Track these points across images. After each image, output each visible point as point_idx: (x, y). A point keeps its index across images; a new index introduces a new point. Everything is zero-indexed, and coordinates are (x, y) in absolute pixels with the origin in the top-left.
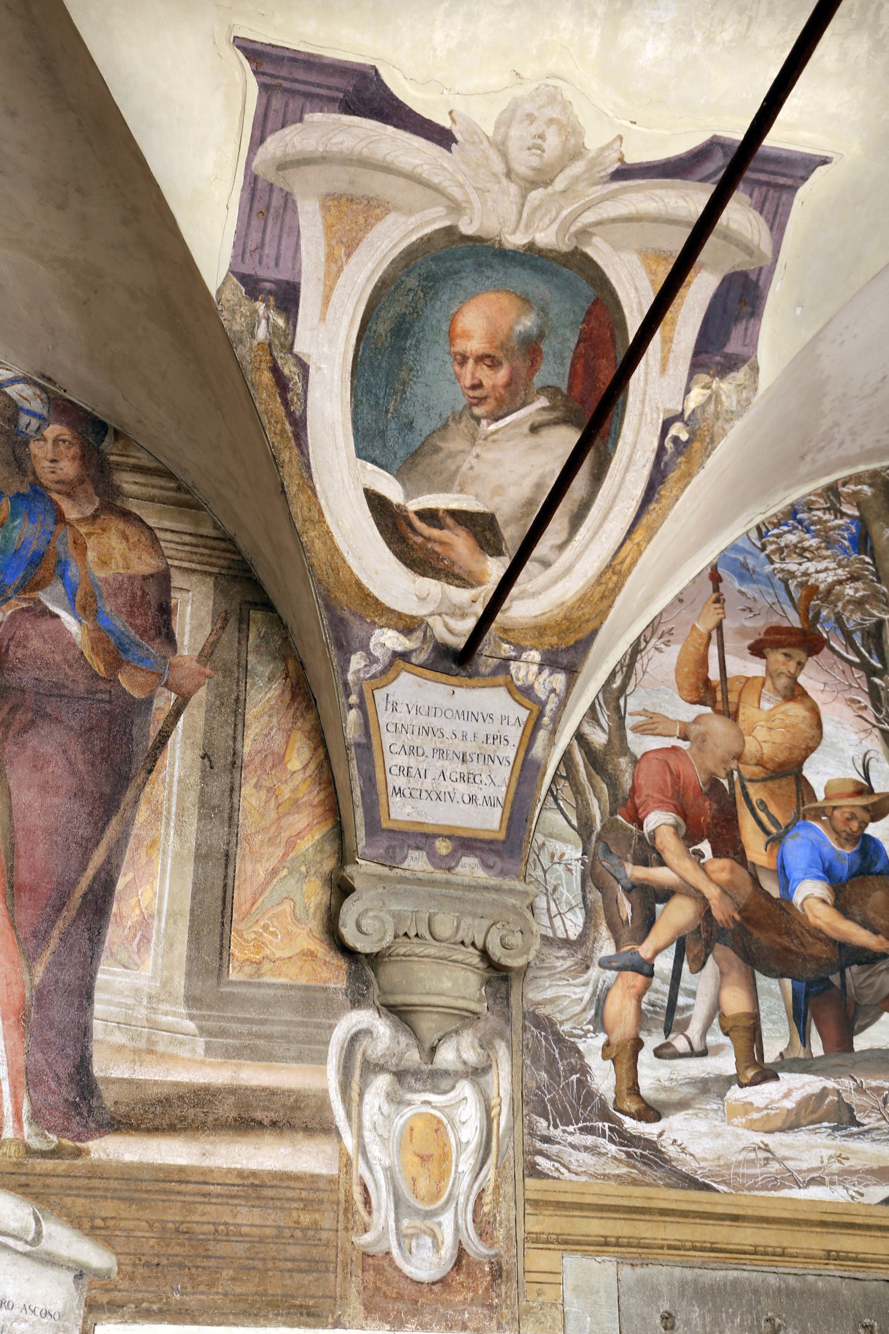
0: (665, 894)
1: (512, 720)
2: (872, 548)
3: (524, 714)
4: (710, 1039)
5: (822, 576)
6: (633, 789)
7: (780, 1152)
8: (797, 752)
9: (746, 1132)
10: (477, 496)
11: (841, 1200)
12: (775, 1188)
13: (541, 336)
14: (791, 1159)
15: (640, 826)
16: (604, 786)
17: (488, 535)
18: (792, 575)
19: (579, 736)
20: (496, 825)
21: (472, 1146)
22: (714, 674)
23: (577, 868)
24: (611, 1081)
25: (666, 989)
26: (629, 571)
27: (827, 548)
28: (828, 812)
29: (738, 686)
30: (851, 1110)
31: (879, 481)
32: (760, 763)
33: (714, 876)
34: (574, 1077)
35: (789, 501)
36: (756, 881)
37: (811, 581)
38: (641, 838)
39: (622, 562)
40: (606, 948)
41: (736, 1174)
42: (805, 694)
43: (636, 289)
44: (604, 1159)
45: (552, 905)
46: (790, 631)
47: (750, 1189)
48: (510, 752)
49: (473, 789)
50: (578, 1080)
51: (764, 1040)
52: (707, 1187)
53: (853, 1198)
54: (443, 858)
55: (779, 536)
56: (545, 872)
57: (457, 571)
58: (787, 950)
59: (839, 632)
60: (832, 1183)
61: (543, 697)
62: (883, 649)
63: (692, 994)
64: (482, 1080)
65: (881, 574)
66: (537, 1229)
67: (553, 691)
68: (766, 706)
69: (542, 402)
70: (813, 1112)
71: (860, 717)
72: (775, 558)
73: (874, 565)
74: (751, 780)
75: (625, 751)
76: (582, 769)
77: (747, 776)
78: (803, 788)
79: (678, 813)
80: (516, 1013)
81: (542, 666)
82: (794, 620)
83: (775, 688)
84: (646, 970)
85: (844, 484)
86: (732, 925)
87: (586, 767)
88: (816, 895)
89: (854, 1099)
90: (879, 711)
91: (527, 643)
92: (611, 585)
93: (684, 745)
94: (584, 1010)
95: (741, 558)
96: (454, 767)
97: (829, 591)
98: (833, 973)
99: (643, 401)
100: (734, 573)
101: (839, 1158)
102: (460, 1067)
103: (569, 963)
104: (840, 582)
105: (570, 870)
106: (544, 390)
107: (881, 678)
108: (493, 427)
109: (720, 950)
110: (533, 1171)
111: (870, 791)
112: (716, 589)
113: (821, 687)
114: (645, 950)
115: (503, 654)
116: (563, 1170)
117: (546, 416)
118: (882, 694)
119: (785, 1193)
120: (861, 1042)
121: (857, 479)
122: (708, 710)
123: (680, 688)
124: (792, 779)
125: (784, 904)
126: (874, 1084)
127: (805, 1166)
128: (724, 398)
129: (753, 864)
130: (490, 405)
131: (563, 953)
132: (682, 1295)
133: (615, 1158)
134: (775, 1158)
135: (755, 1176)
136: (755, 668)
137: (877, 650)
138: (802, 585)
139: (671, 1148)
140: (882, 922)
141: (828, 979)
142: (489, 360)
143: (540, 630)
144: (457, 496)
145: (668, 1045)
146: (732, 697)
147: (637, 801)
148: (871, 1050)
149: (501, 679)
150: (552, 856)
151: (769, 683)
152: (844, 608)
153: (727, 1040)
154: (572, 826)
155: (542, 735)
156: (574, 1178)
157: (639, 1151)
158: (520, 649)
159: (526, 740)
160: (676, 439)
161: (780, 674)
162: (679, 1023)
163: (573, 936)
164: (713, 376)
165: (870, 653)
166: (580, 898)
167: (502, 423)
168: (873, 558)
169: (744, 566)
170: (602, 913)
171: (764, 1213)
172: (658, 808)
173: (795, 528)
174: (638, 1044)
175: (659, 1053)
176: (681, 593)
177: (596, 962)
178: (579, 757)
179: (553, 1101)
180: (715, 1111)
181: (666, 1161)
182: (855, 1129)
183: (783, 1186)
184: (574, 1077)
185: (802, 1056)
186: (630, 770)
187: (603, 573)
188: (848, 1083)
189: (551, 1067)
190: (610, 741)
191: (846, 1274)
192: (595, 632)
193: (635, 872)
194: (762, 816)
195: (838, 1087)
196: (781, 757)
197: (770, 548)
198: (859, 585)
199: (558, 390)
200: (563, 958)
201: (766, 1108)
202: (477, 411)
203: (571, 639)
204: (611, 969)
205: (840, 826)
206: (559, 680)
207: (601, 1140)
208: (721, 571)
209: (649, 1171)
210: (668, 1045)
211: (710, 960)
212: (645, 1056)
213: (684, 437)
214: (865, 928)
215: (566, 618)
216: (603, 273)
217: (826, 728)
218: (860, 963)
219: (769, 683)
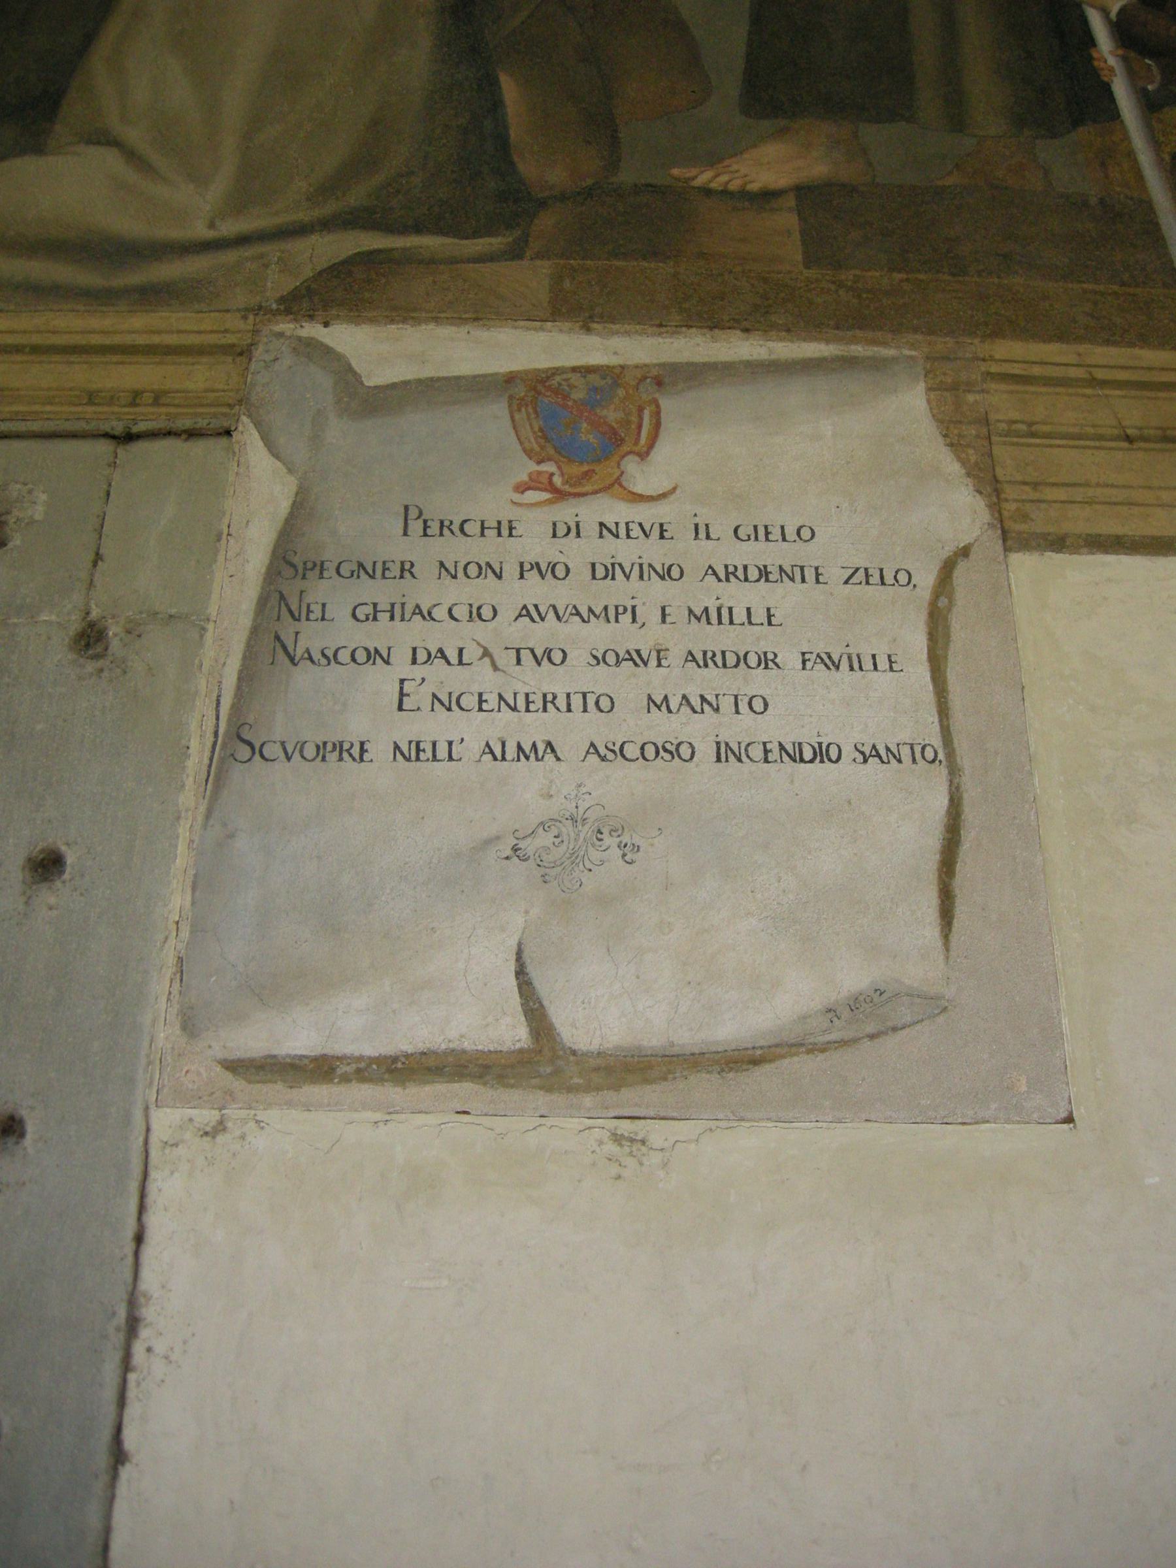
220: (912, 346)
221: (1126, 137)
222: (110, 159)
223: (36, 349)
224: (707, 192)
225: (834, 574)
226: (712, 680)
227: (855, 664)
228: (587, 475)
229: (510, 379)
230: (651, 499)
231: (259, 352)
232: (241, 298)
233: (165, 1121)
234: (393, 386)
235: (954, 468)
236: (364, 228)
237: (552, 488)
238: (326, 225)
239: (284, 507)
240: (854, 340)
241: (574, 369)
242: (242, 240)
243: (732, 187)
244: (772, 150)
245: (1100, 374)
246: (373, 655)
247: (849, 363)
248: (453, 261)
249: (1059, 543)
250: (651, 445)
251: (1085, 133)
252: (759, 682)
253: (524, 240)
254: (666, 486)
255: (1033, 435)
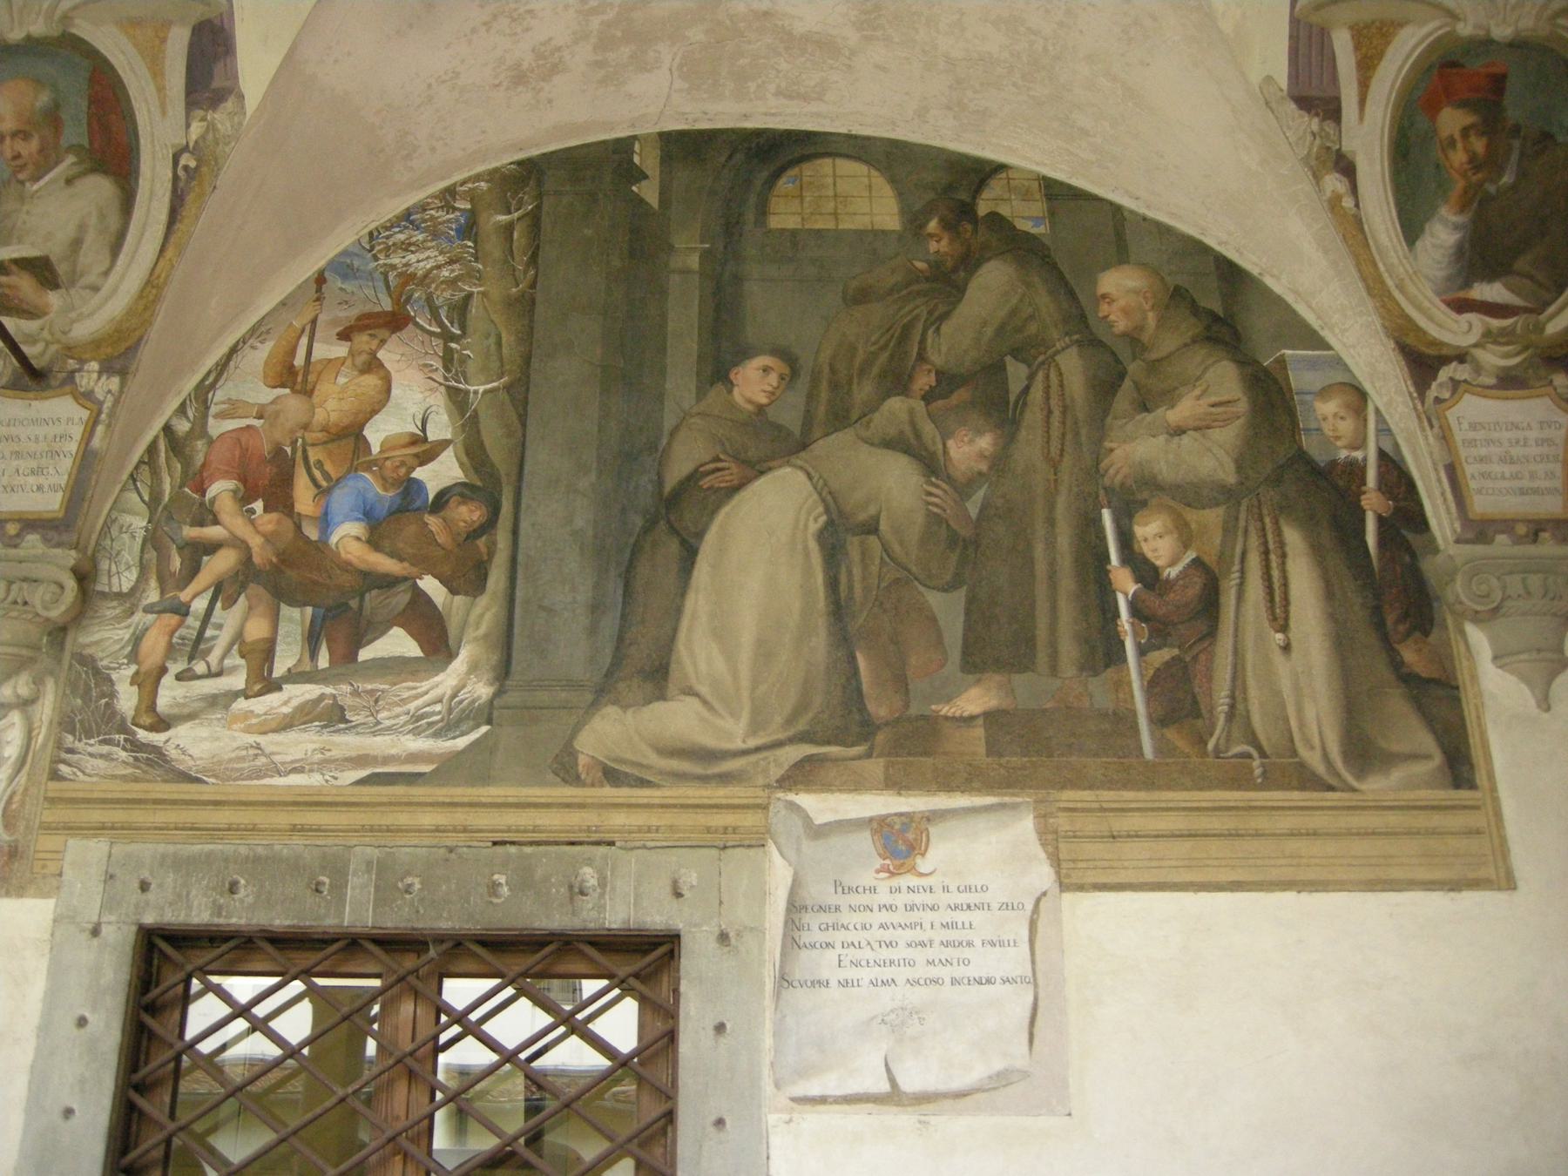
0: (212, 548)
1: (76, 420)
2: (476, 234)
3: (85, 414)
4: (227, 662)
5: (422, 264)
6: (203, 465)
7: (268, 750)
8: (361, 416)
9: (242, 734)
10: (32, 244)
11: (316, 784)
12: (259, 778)
13: (57, 106)
14: (279, 753)
15: (203, 495)
16: (179, 466)
17: (47, 274)
18: (393, 267)
19: (167, 429)
20: (57, 506)
21: (12, 760)
22: (299, 361)
23: (140, 534)
24: (134, 701)
25: (197, 624)
26: (165, 283)
27: (433, 240)
28: (380, 463)
29: (319, 367)
30: (342, 709)
31: (497, 176)
32: (325, 429)
33: (261, 528)
34: (103, 701)
35: (405, 206)
36: (298, 527)
37: (412, 270)
38: (202, 504)
39: (159, 277)
40: (153, 596)
41: (227, 769)
42: (381, 365)
43: (123, 52)
44: (113, 764)
45: (113, 567)
46: (378, 314)
47: (235, 780)
48: (73, 447)
49: (41, 480)
50: (107, 704)
51: (276, 659)
52: (198, 780)
53: (327, 781)
54: (11, 537)
55: (388, 237)
56: (112, 540)
57: (25, 307)
58: (315, 583)
59: (427, 309)
60: (311, 771)
61: (102, 398)
62: (465, 318)
63: (220, 627)
64: (30, 709)
65: (480, 255)
66: (50, 819)
67: (109, 391)
68: (342, 380)
69: (71, 159)
70: (307, 714)
71: (430, 378)
72: (381, 256)
73: (475, 248)
74: (313, 445)
75: (204, 433)
76: (163, 455)
77: (309, 441)
78: (361, 443)
79: (240, 480)
80: (67, 657)
81: (100, 373)
82: (387, 305)
83: (354, 365)
84: (183, 611)
85: (462, 185)
86: (268, 568)
87: (166, 452)
88: (353, 534)
89: (348, 701)
90: (447, 369)
91: (87, 356)
92: (151, 298)
93: (257, 423)
94: (123, 648)
95: (349, 261)
96: (26, 464)
97: (426, 276)
98: (353, 598)
99: (153, 141)
100: (339, 275)
101: (322, 750)
102: (13, 700)
103: (117, 611)
104: (438, 267)
105: (134, 537)
106: (71, 149)
107: (457, 343)
108: (35, 187)
109: (254, 589)
110: (55, 776)
111: (425, 439)
112: (319, 290)
113: (398, 357)
114: (184, 596)
115: (70, 368)
116: (79, 773)
117: (76, 170)
118: (456, 356)
119: (267, 781)
120: (365, 654)
121: (477, 178)
122: (287, 391)
123: (265, 377)
124: (351, 440)
125: (321, 546)
126: (369, 687)
127: (289, 758)
128: (219, 126)
129: (299, 514)
130: (31, 167)
131: (115, 603)
132: (162, 865)
133: (124, 762)
134: (264, 754)
135: (243, 769)
136: (340, 350)
137: (459, 320)
138: (400, 275)
139: (173, 752)
140: (410, 551)
141: (347, 604)
142: (22, 134)
143: (96, 344)
144: (16, 247)
145: (189, 670)
146: (311, 378)
147: (205, 474)
148: (373, 660)
149: (68, 388)
150: (121, 527)
151: (349, 362)
152: (436, 289)
153: (243, 662)
154: (143, 501)
155: (100, 429)
156: (87, 779)
157: (145, 755)
158: (82, 361)
159: (87, 435)
160: (186, 168)
161: (360, 353)
162: (203, 651)
163: (125, 589)
164: (207, 110)
165: (452, 324)
166: (137, 559)
167: (42, 183)
168: (475, 242)
169: (350, 266)
170: (154, 570)
171: (243, 798)
172: (223, 478)
173: (406, 228)
174: (163, 670)
175: (179, 677)
176: (286, 298)
177: (141, 608)
178: (162, 446)
179: (81, 722)
180: (219, 719)
181: (166, 761)
182: (342, 726)
183: (265, 776)
184: (103, 701)
185: (308, 669)
186: (204, 450)
187: (142, 291)
188: (346, 688)
189: (86, 696)
190: (192, 429)
191: (308, 842)
192: (141, 339)
193: (190, 532)
194: (317, 474)
195: (334, 692)
196: (346, 421)
197: (378, 248)
198: (457, 266)
199: (81, 146)
200: (114, 608)
201: (265, 714)
202: (21, 176)
203: (123, 347)
204: (152, 613)
205: (388, 473)
206: (114, 383)
207: (115, 749)
208: (327, 274)
209: (150, 770)
210: (189, 670)
211: (242, 598)
212: (168, 680)
213: (193, 164)
214: (392, 557)
215: (117, 331)
216: (92, 46)
217: (394, 392)
218: (379, 588)
219: (349, 362)
220: (1029, 796)
221: (1128, 674)
222: (692, 702)
223: (683, 806)
224: (946, 718)
225: (995, 906)
226: (949, 952)
227: (1002, 944)
228: (902, 865)
229: (871, 820)
230: (927, 875)
231: (771, 808)
232: (761, 781)
233: (772, 1119)
234: (826, 824)
235: (1043, 855)
236: (806, 742)
237: (889, 872)
238: (791, 741)
239: (789, 880)
240: (1005, 795)
241: (896, 814)
242: (758, 749)
243: (957, 714)
244: (974, 692)
245: (1105, 805)
246: (828, 945)
247: (1003, 806)
248: (845, 759)
249: (1081, 888)
250: (926, 850)
251: (1110, 673)
252: (966, 953)
253: (871, 748)
254: (932, 869)
255: (1075, 837)
